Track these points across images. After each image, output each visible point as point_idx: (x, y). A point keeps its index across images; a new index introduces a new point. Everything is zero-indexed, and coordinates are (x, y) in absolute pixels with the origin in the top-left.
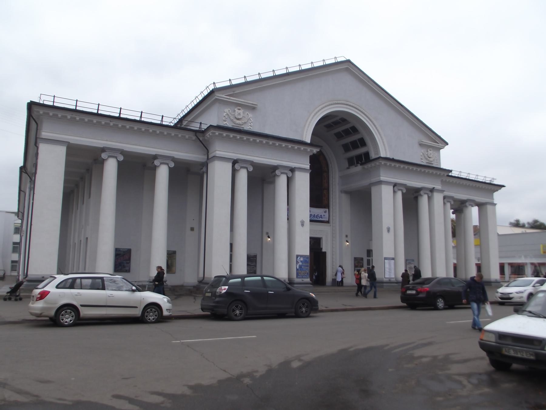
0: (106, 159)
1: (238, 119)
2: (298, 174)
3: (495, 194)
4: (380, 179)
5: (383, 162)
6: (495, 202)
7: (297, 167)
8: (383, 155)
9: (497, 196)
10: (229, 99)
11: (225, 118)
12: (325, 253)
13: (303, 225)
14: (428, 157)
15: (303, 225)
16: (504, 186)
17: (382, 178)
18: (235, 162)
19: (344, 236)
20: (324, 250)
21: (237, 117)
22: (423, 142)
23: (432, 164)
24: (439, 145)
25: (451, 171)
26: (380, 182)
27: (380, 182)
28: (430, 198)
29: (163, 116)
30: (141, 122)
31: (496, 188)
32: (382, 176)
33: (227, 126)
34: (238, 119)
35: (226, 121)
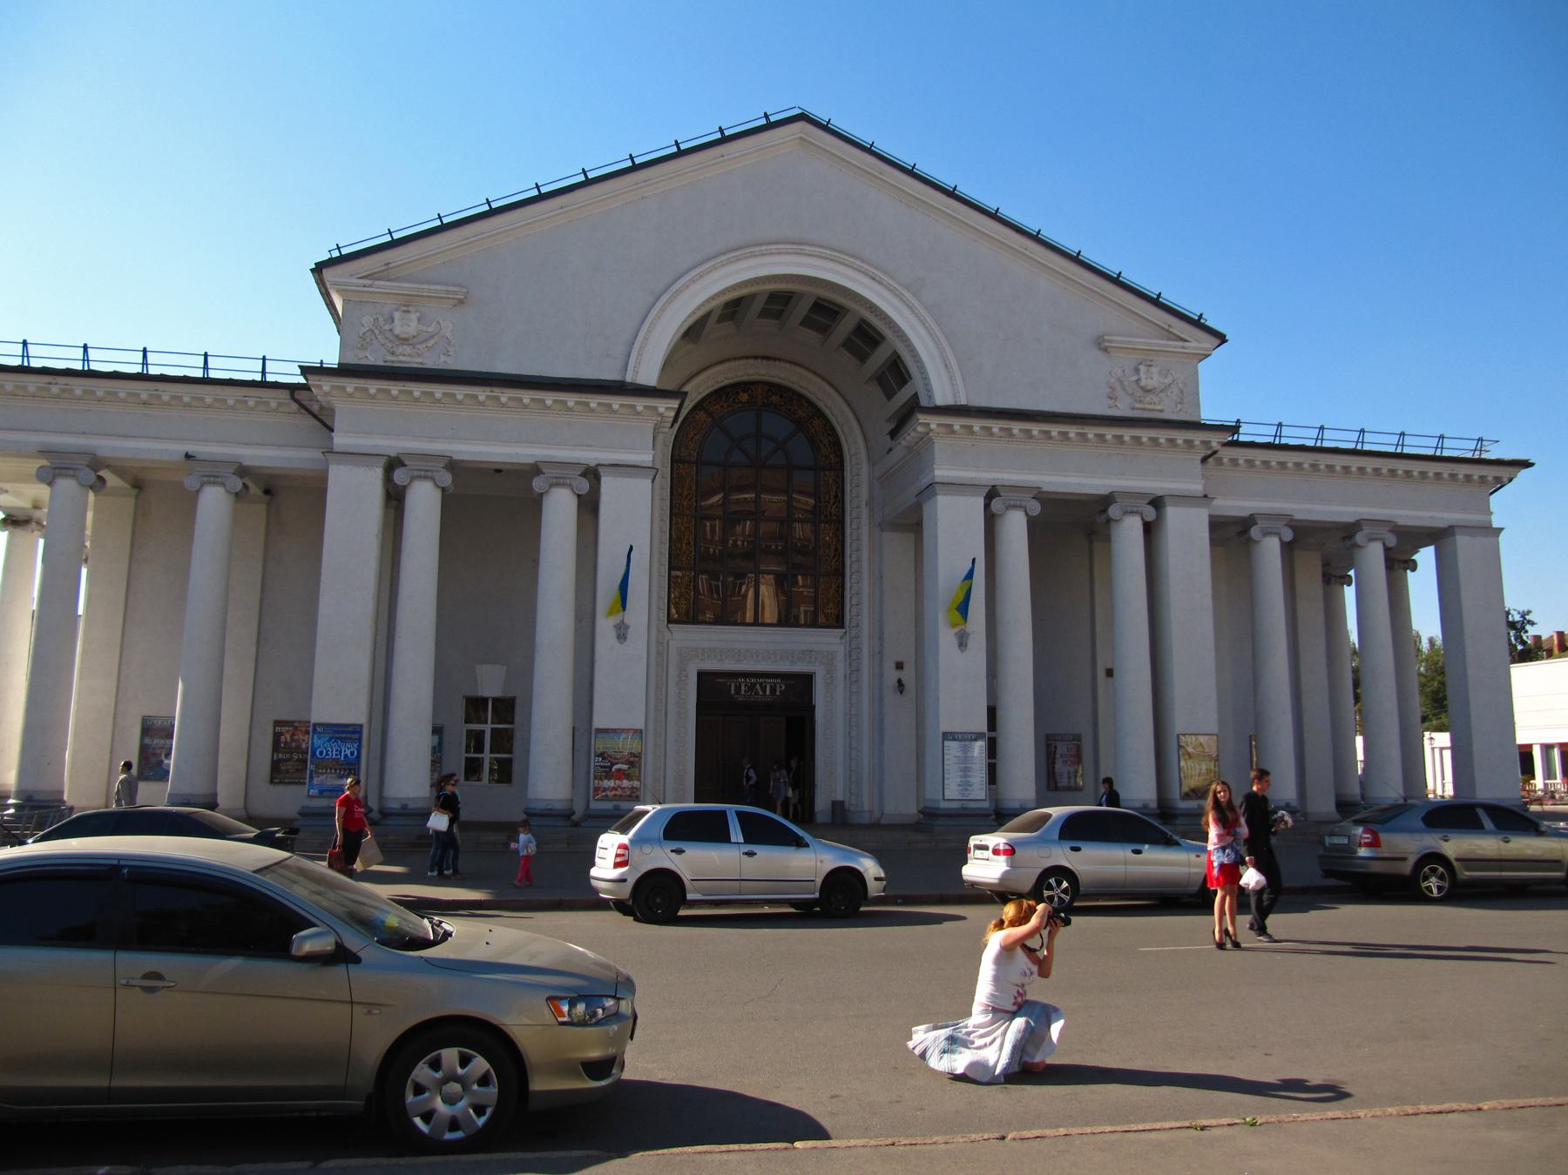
3: (1496, 501)
5: (934, 422)
6: (1495, 524)
7: (606, 463)
8: (942, 397)
9: (1503, 506)
10: (370, 286)
16: (1526, 464)
18: (393, 464)
22: (1110, 341)
23: (1162, 411)
24: (1187, 344)
27: (931, 489)
28: (1150, 530)
29: (145, 351)
30: (206, 381)
31: (1490, 472)
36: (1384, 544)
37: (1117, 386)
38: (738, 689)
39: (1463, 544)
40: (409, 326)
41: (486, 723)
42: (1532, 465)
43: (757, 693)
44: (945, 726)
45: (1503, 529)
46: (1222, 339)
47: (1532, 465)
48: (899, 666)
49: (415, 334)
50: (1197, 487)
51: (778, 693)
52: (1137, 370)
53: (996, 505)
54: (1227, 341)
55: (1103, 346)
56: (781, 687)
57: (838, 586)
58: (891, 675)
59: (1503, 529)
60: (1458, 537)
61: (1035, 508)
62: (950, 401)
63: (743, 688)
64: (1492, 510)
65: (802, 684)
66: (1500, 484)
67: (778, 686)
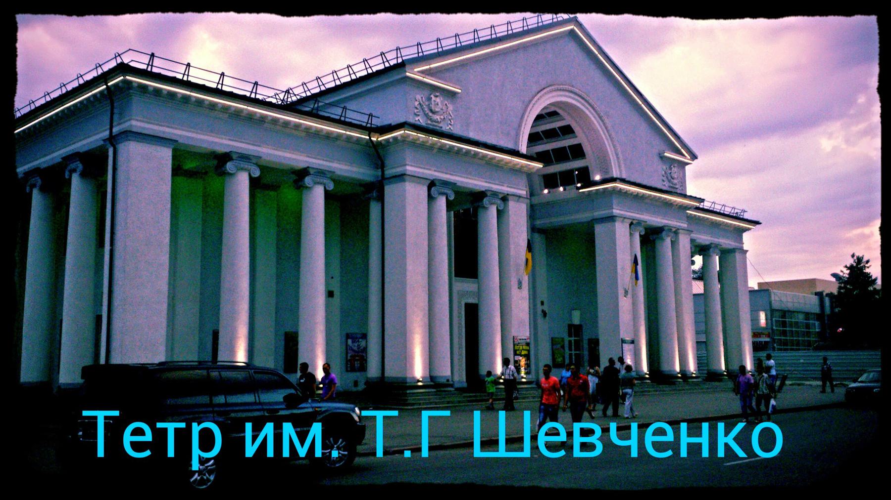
2: (512, 204)
4: (613, 212)
7: (511, 194)
11: (418, 110)
13: (520, 287)
14: (672, 177)
15: (520, 287)
18: (432, 184)
19: (539, 304)
21: (433, 108)
23: (677, 188)
25: (702, 200)
26: (611, 218)
27: (611, 218)
32: (615, 209)
33: (419, 123)
34: (431, 111)
35: (418, 115)
42: (761, 223)
47: (761, 223)
48: (542, 303)
58: (540, 308)
60: (736, 254)
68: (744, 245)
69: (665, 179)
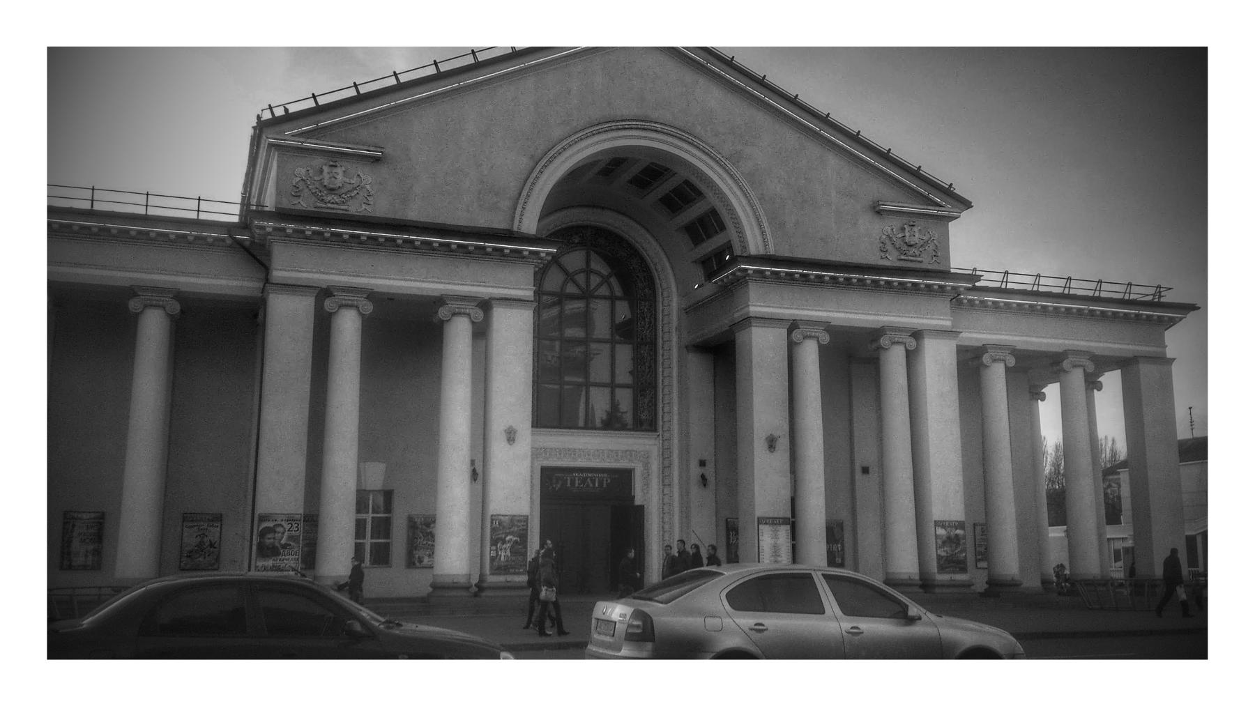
0: (142, 312)
1: (332, 190)
8: (755, 247)
12: (641, 508)
17: (756, 308)
20: (638, 502)
23: (921, 262)
26: (747, 321)
27: (747, 321)
36: (1084, 370)
37: (887, 241)
38: (573, 482)
39: (1146, 371)
40: (336, 178)
41: (368, 513)
42: (1199, 308)
43: (588, 486)
44: (759, 512)
45: (1174, 359)
46: (967, 205)
47: (1199, 308)
49: (341, 185)
50: (946, 323)
51: (605, 486)
52: (903, 229)
53: (796, 335)
54: (972, 206)
55: (877, 209)
56: (607, 481)
57: (652, 398)
59: (1174, 359)
61: (825, 338)
62: (762, 252)
63: (577, 482)
64: (1166, 344)
65: (623, 478)
66: (1172, 322)
67: (605, 479)
68: (1167, 350)
69: (889, 247)
